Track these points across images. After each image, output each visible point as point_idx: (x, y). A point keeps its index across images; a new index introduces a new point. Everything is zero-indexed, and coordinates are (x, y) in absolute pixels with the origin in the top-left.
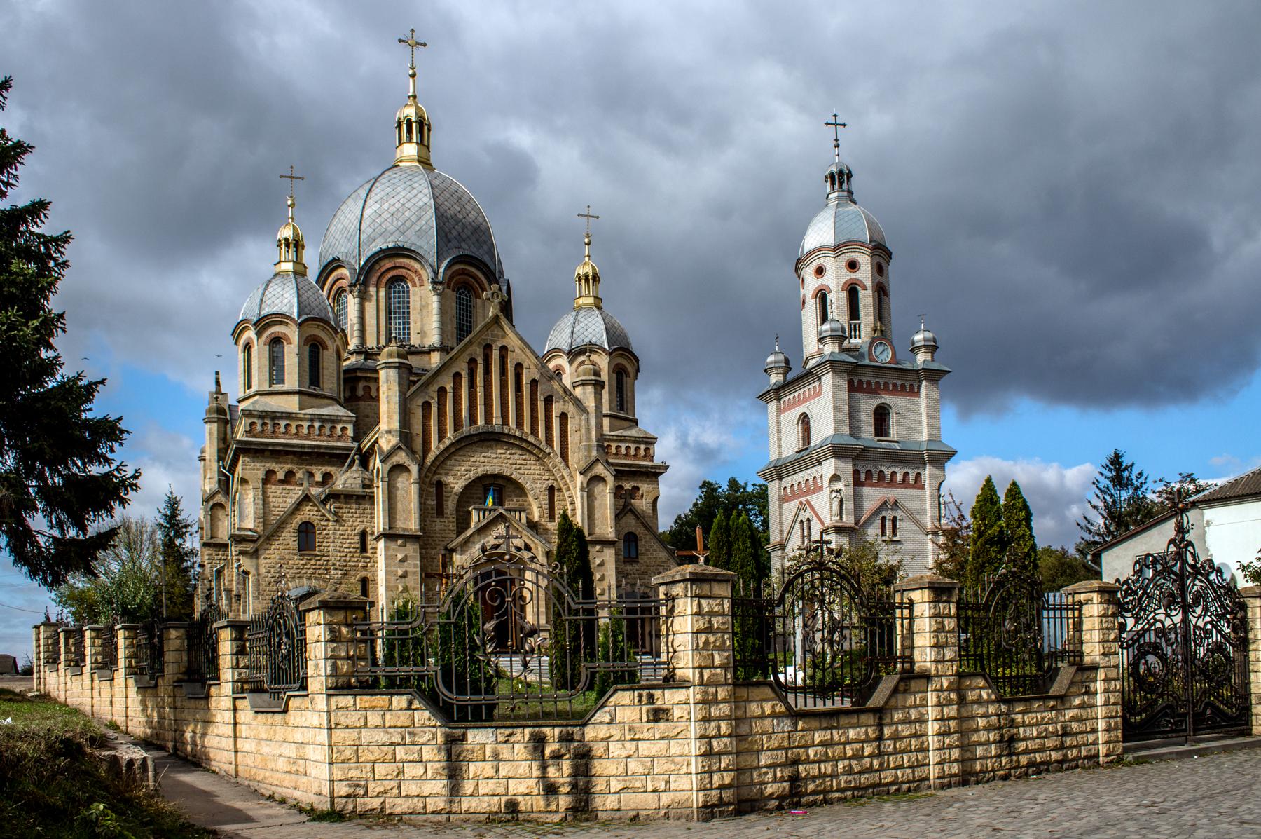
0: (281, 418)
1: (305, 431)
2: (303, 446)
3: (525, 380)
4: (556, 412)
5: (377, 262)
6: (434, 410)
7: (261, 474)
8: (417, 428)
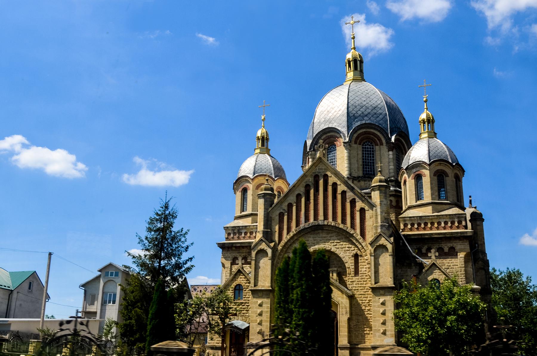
4: (358, 208)
6: (286, 218)
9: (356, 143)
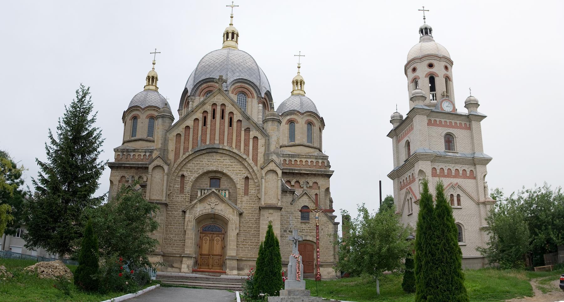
0: (131, 152)
1: (142, 157)
2: (138, 164)
3: (235, 120)
4: (252, 136)
5: (200, 86)
7: (118, 178)
8: (171, 146)
9: (232, 93)
